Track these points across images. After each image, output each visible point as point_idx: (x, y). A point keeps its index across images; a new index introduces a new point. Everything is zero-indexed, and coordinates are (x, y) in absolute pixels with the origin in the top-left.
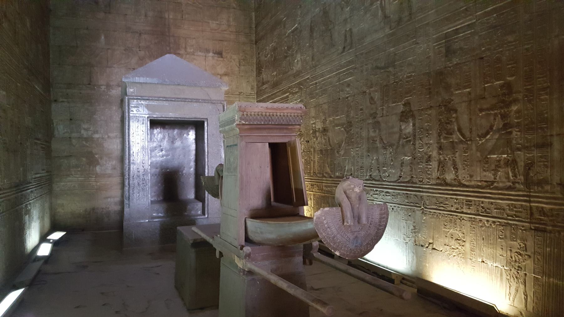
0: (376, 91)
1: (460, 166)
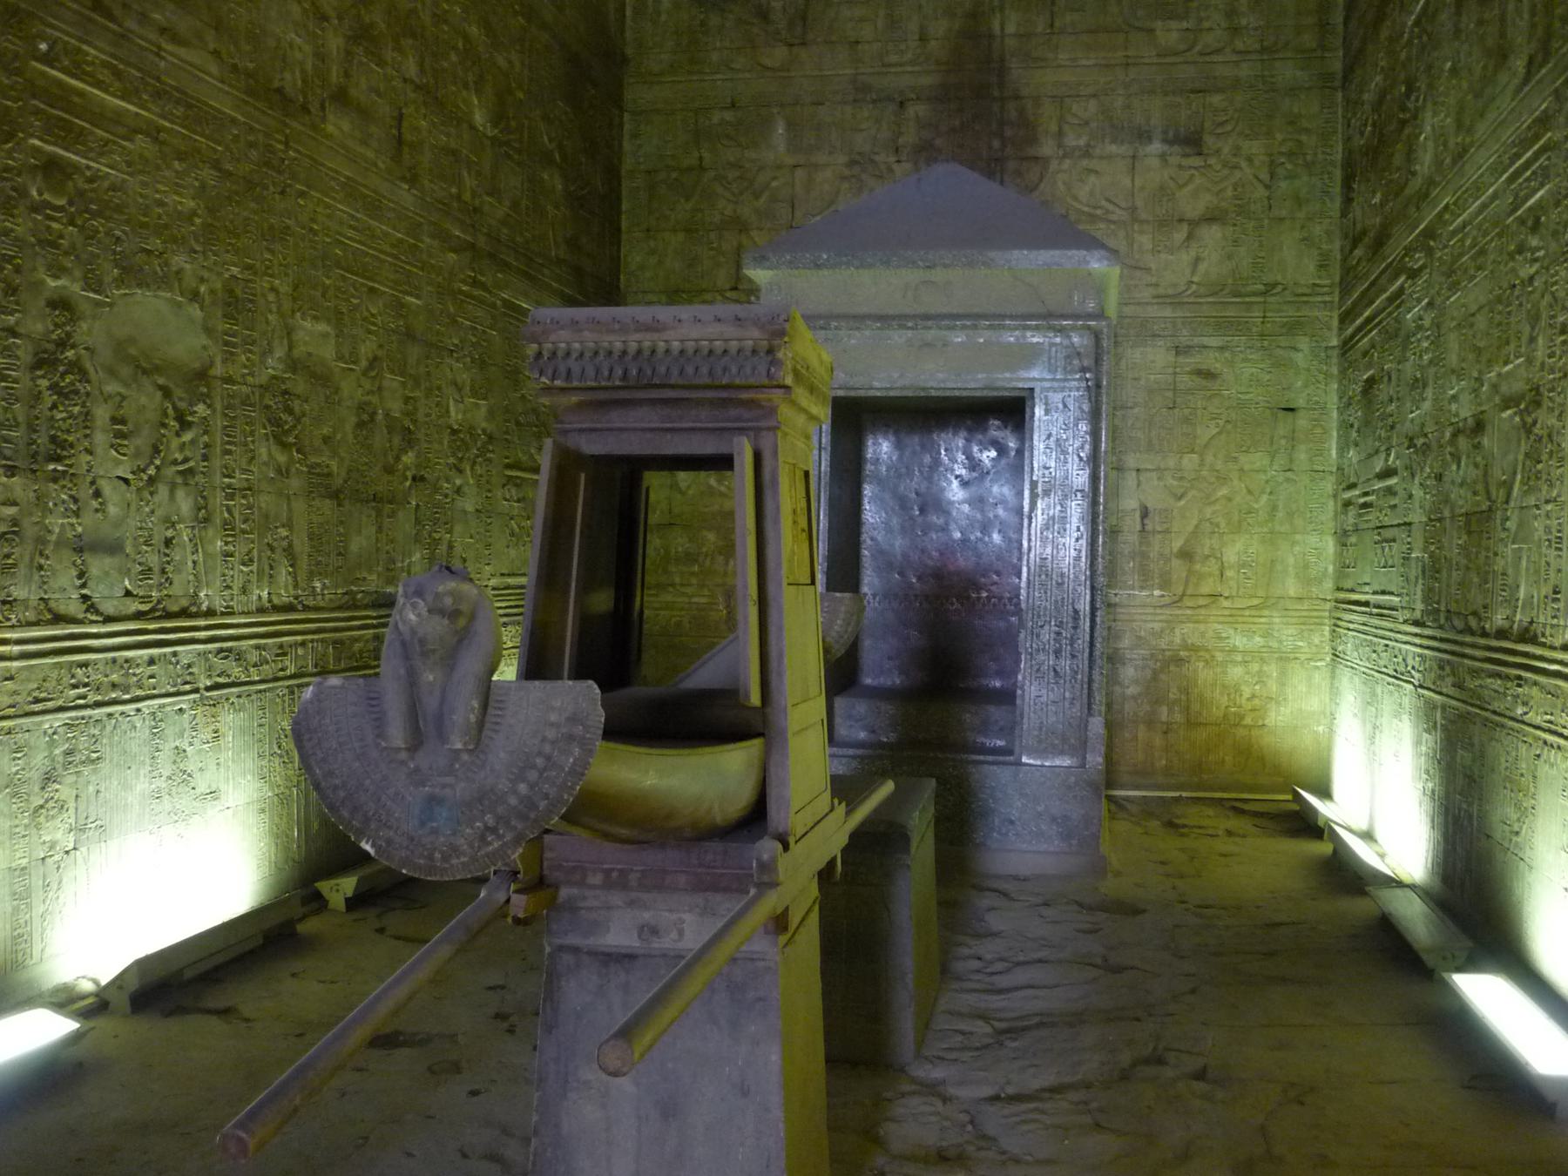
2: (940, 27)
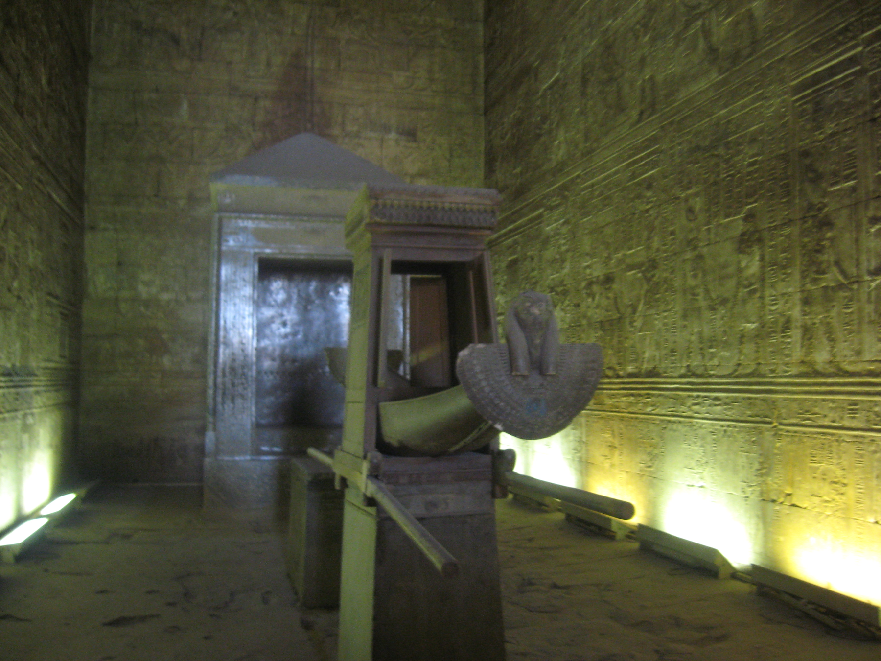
0: (696, 195)
1: (839, 335)
2: (278, 60)
